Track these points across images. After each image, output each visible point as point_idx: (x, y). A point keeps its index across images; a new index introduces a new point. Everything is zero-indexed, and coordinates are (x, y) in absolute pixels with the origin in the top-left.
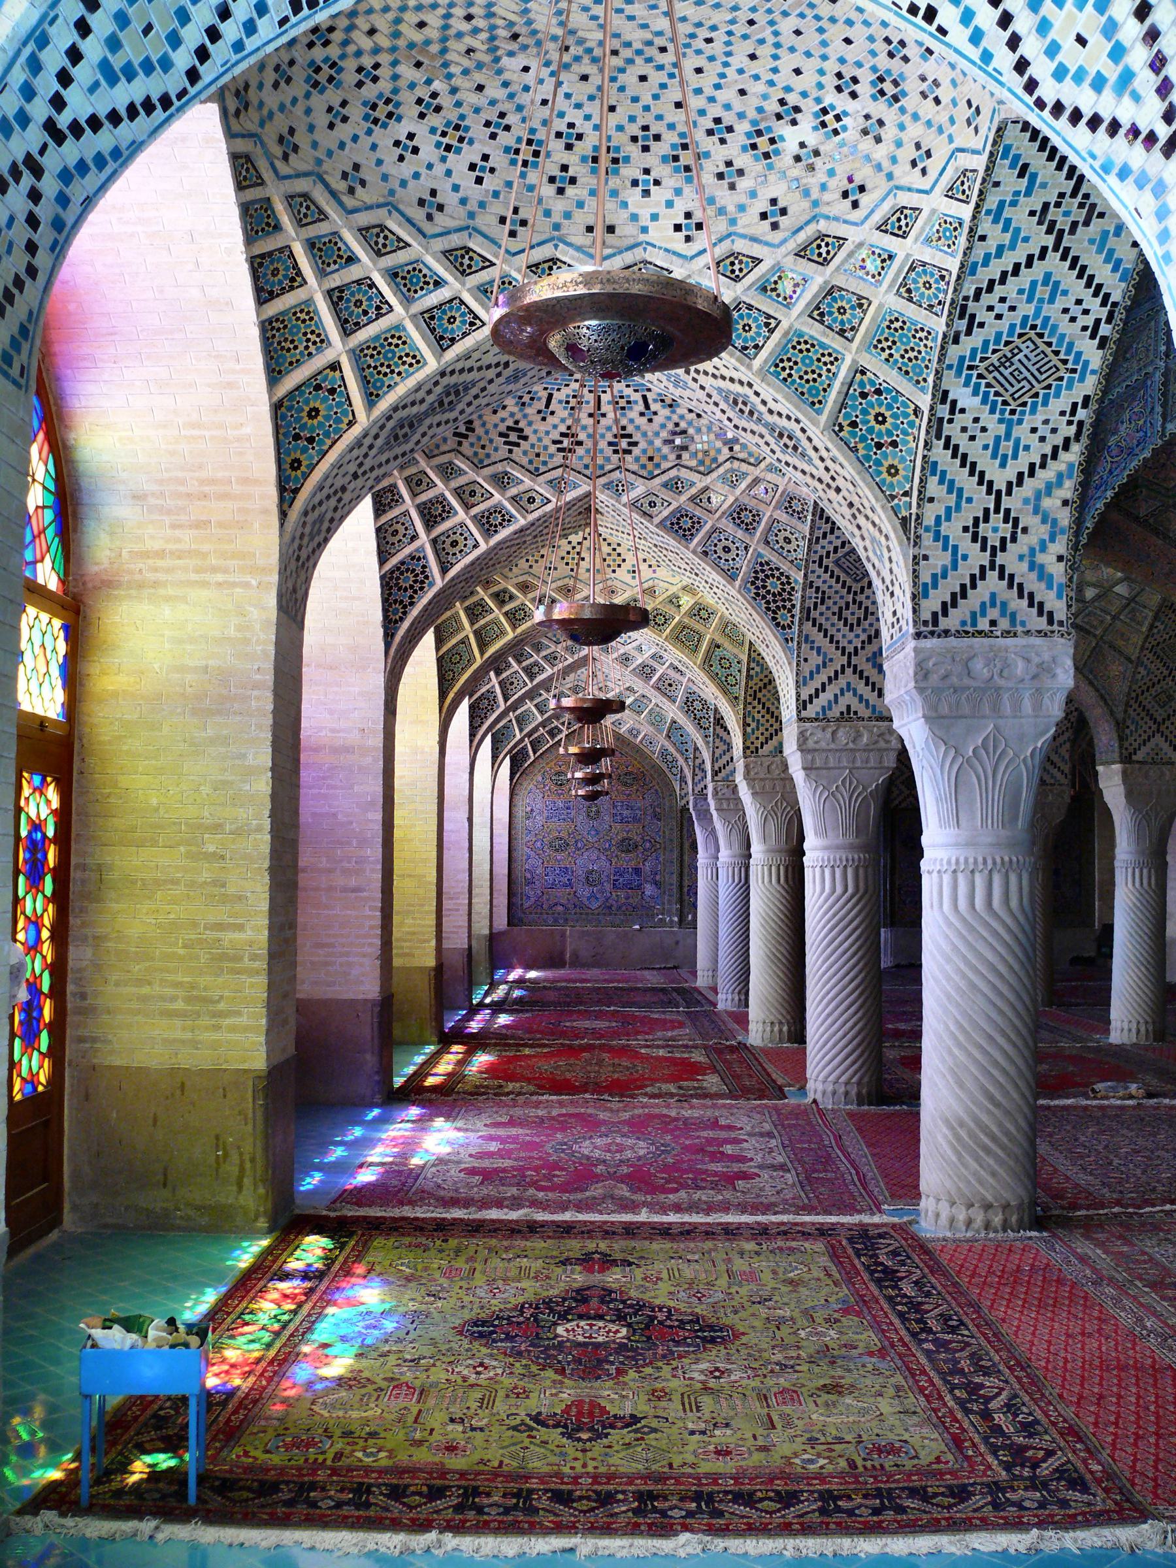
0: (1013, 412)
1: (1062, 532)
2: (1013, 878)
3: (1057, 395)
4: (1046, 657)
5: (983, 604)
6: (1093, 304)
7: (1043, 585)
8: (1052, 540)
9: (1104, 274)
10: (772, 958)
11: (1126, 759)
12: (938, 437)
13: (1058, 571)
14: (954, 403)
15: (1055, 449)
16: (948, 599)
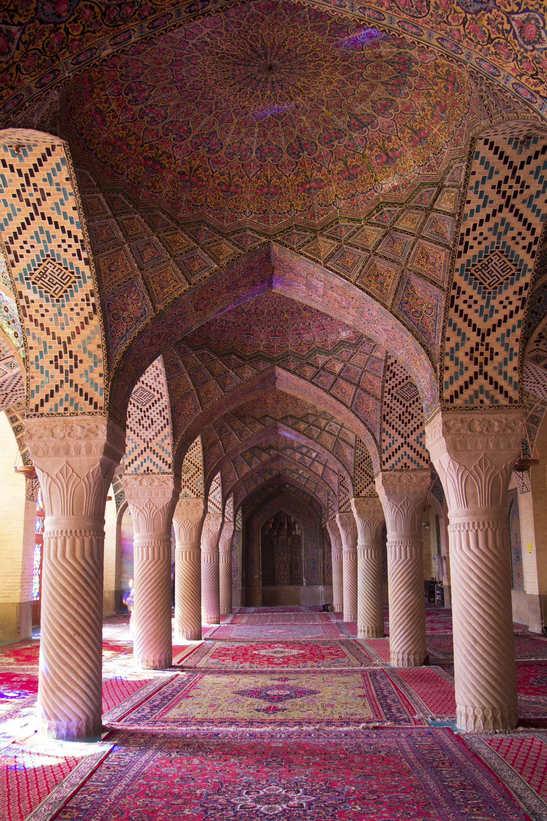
0: (58, 301)
1: (100, 362)
2: (78, 542)
3: (77, 291)
4: (93, 425)
5: (62, 400)
6: (72, 241)
7: (93, 389)
8: (96, 366)
9: (68, 226)
10: (183, 598)
11: (357, 496)
12: (25, 315)
13: (100, 381)
14: (26, 297)
15: (86, 318)
16: (44, 398)
